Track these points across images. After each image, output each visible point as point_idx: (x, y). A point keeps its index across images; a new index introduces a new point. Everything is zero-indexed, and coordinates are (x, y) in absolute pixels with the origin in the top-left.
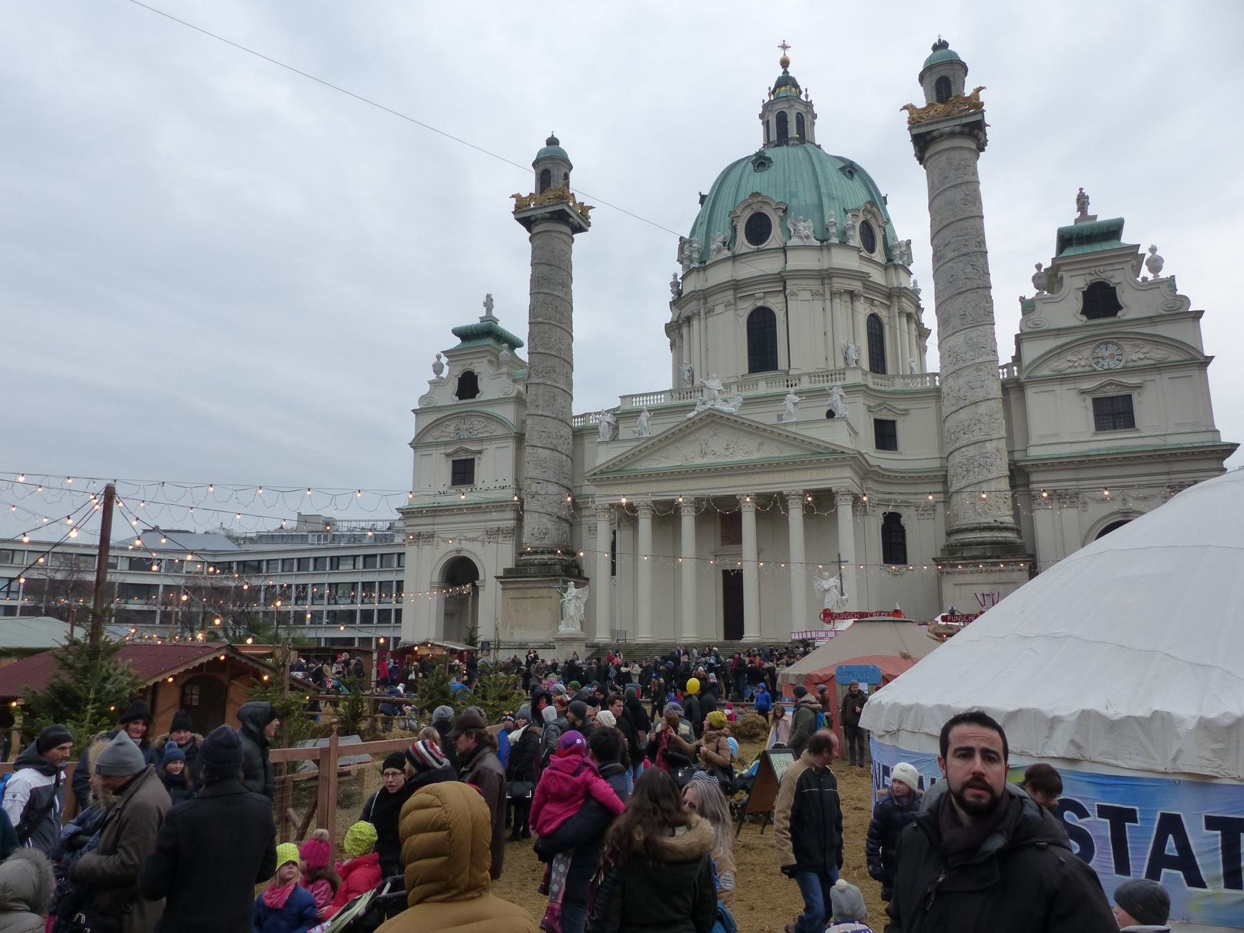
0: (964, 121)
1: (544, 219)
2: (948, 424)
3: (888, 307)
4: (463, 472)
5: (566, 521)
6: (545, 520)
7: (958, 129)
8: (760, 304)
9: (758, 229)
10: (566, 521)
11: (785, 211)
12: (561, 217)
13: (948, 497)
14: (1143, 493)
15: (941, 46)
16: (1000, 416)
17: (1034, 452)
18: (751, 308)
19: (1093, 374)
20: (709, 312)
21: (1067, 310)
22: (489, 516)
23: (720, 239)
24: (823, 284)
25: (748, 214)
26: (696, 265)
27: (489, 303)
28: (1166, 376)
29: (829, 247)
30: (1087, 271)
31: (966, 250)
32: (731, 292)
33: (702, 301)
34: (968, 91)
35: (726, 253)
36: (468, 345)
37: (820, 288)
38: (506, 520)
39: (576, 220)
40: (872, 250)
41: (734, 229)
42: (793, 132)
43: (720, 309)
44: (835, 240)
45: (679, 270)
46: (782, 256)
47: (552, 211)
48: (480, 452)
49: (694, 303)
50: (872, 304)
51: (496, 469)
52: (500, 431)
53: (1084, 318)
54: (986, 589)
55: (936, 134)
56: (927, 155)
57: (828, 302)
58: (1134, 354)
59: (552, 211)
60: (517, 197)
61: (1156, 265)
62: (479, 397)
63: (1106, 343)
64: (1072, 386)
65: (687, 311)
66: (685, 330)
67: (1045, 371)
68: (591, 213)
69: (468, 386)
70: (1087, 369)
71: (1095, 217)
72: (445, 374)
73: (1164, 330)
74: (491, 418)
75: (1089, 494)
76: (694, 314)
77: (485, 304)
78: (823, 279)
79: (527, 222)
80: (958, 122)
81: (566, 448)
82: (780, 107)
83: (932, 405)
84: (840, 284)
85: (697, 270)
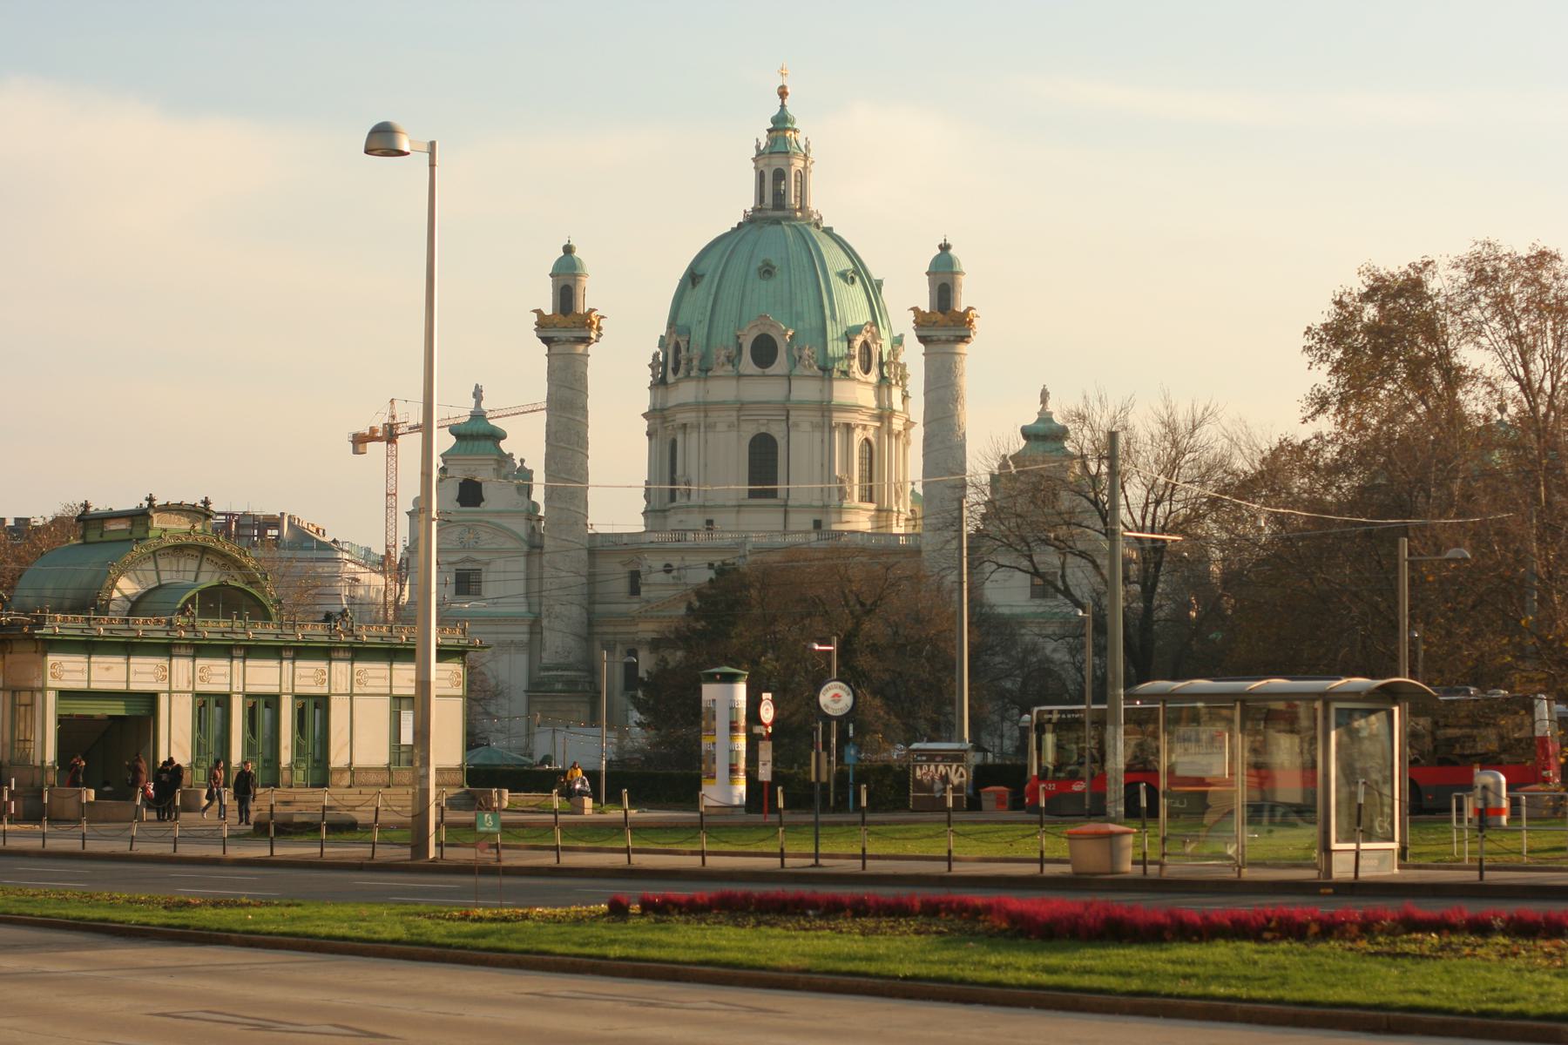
8: (763, 430)
18: (755, 432)
20: (710, 427)
22: (500, 629)
25: (755, 333)
27: (478, 394)
29: (831, 379)
34: (961, 307)
37: (818, 419)
38: (521, 634)
41: (740, 347)
43: (721, 427)
46: (786, 382)
47: (566, 326)
51: (505, 585)
59: (566, 326)
60: (539, 312)
69: (470, 493)
74: (499, 529)
76: (692, 426)
82: (778, 162)
85: (698, 378)
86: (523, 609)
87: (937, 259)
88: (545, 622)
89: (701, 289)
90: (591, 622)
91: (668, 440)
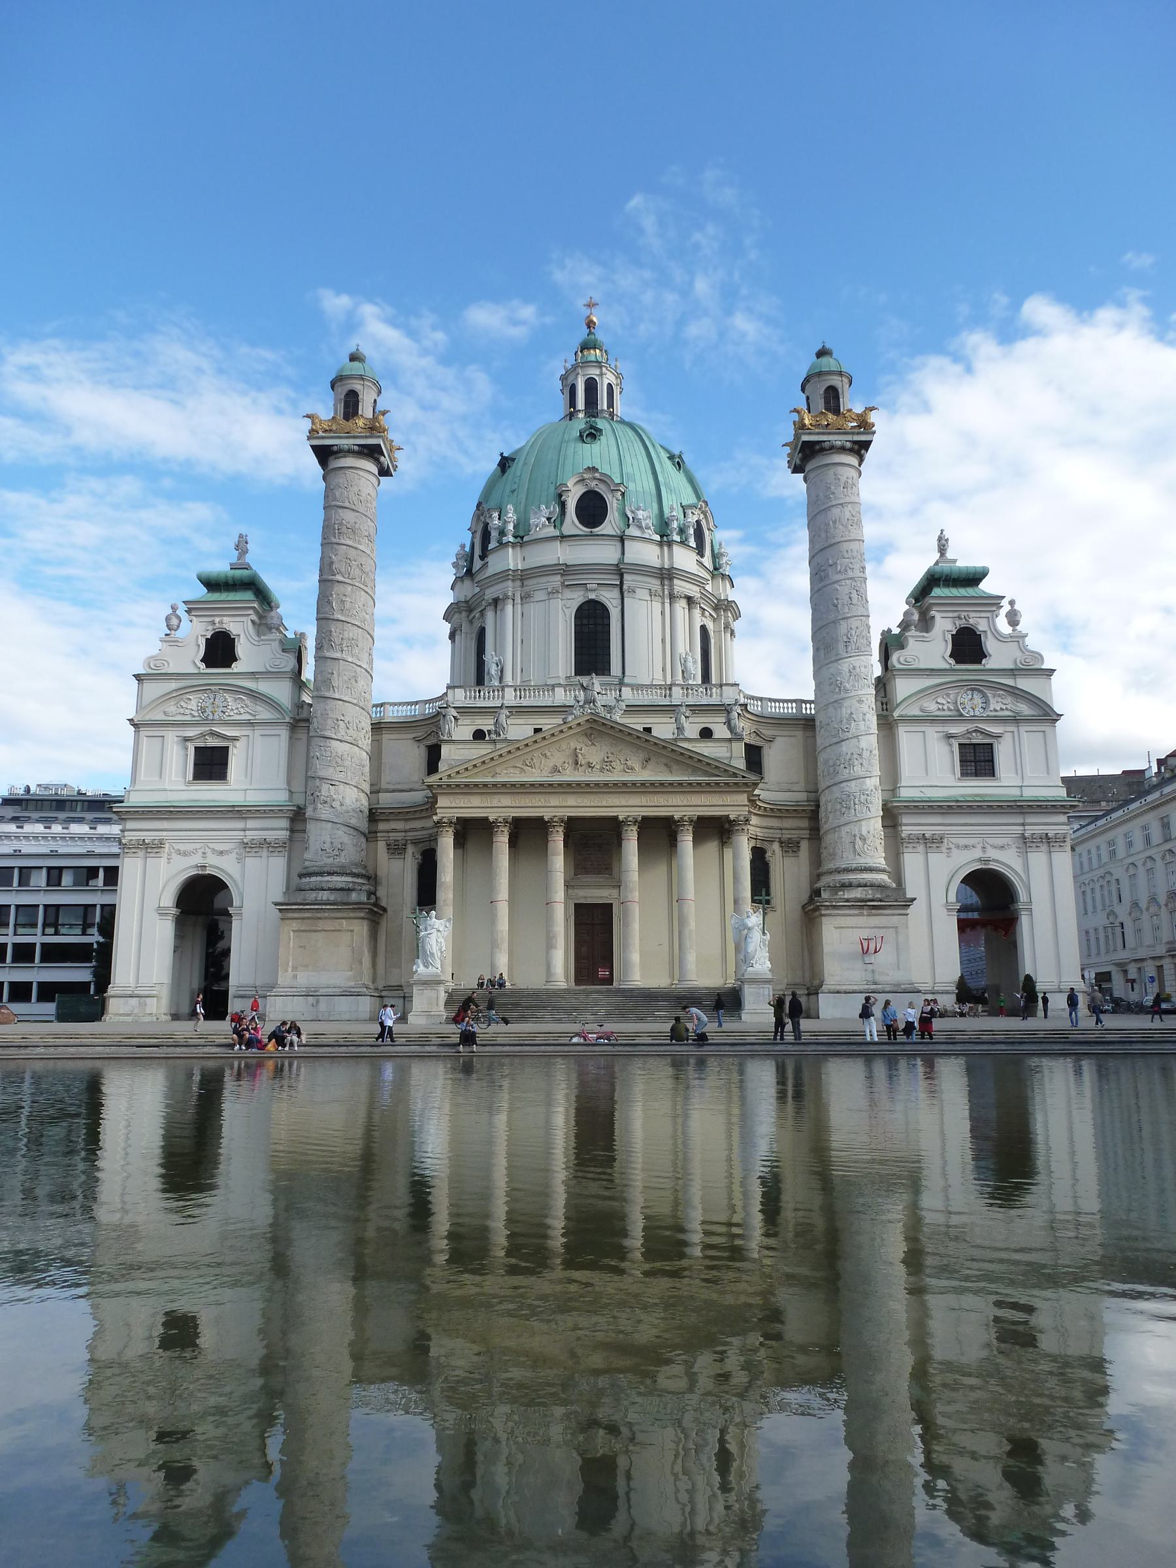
0: (856, 438)
1: (350, 452)
2: (821, 758)
3: (714, 620)
4: (211, 763)
5: (364, 834)
6: (340, 833)
7: (848, 445)
8: (592, 596)
9: (592, 509)
10: (364, 834)
11: (623, 494)
12: (372, 452)
13: (815, 833)
14: (1000, 842)
15: (822, 353)
16: (876, 752)
17: (905, 793)
19: (959, 718)
20: (526, 598)
21: (932, 649)
22: (251, 824)
23: (545, 511)
24: (662, 585)
26: (511, 539)
28: (1024, 728)
29: (670, 544)
30: (956, 614)
31: (850, 574)
32: (558, 578)
33: (518, 583)
35: (551, 531)
36: (216, 596)
37: (659, 588)
38: (278, 830)
39: (385, 461)
40: (702, 556)
41: (563, 505)
42: (603, 404)
43: (540, 595)
44: (677, 538)
45: (467, 538)
46: (619, 545)
48: (235, 739)
49: (510, 583)
50: (703, 615)
52: (264, 713)
53: (952, 661)
54: (865, 934)
55: (826, 445)
56: (807, 469)
57: (667, 605)
58: (999, 704)
61: (1013, 618)
62: (236, 667)
63: (973, 690)
64: (940, 729)
65: (490, 594)
66: (490, 615)
67: (915, 711)
68: (397, 454)
69: (220, 650)
70: (954, 713)
71: (955, 561)
72: (178, 634)
73: (1024, 684)
74: (254, 695)
75: (955, 840)
77: (237, 547)
78: (662, 579)
79: (324, 454)
80: (850, 438)
81: (366, 741)
83: (799, 734)
84: (681, 587)
85: (514, 545)
86: (281, 797)
87: (813, 366)
88: (309, 812)
89: (515, 470)
90: (374, 816)
91: (474, 635)
